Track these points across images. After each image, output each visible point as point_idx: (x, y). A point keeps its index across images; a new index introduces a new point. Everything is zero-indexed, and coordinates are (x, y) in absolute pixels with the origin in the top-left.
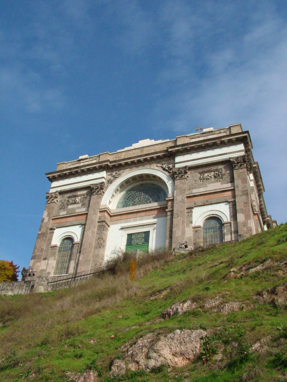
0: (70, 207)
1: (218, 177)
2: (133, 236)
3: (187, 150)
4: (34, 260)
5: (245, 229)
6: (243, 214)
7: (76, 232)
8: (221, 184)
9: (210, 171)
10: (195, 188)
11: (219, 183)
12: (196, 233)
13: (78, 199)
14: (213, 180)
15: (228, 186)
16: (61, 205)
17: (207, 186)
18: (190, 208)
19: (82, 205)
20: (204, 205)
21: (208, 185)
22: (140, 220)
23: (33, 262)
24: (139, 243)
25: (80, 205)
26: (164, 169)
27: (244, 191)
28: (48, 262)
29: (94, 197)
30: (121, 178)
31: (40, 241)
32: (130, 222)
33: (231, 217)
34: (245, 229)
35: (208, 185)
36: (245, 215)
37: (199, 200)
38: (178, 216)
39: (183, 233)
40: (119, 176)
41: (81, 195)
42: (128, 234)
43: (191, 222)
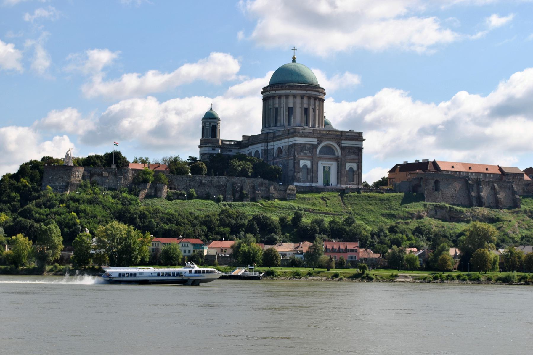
0: (304, 152)
1: (354, 153)
7: (308, 163)
9: (351, 149)
11: (354, 156)
22: (328, 161)
25: (308, 152)
26: (337, 144)
33: (357, 169)
37: (348, 161)
39: (344, 172)
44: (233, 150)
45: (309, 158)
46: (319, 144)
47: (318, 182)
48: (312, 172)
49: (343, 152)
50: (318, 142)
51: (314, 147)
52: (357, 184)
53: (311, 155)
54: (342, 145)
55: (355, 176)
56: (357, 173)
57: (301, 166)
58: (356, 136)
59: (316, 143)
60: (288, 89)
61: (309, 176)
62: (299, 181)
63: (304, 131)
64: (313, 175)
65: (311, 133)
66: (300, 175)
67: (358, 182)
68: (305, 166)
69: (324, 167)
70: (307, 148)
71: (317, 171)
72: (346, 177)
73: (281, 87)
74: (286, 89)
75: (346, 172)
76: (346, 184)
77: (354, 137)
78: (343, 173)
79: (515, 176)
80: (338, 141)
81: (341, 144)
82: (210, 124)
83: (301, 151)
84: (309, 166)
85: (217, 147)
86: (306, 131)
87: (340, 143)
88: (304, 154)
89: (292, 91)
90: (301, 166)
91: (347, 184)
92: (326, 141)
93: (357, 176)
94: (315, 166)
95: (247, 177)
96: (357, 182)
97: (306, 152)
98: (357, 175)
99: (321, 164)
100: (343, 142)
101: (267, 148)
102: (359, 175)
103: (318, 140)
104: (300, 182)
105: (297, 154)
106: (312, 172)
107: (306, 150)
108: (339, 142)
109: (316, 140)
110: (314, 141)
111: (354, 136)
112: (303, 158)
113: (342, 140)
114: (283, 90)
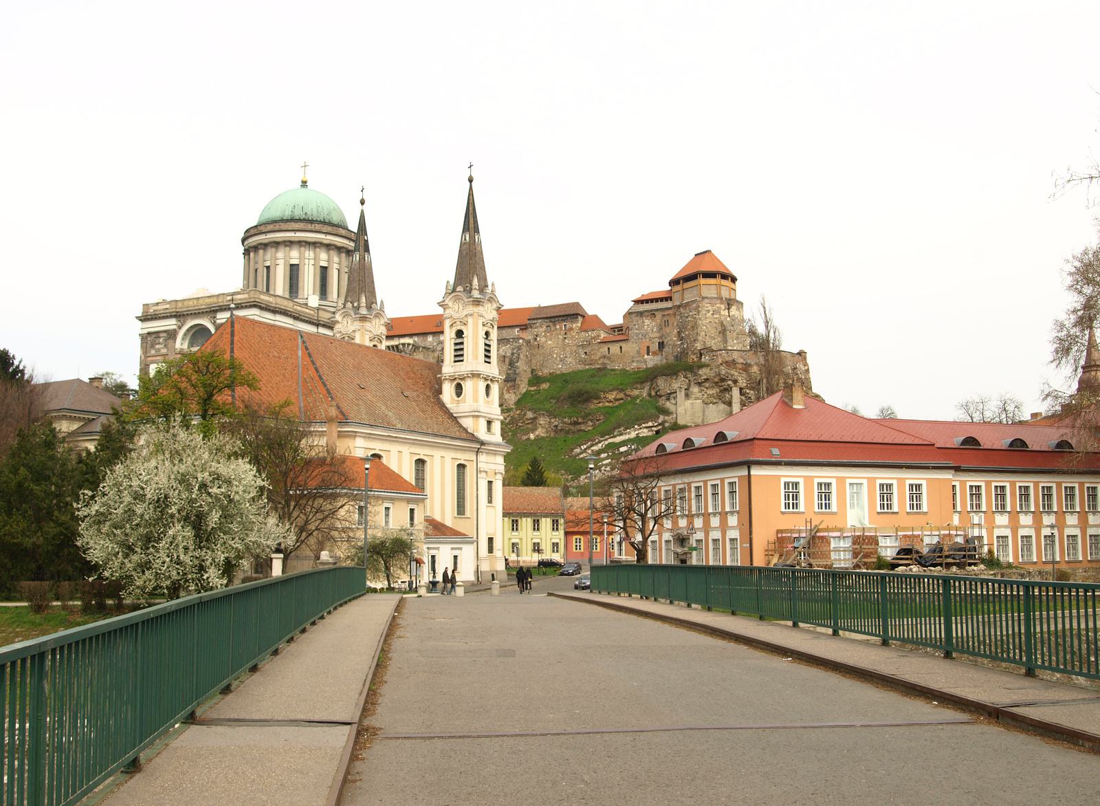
0: (157, 346)
46: (180, 328)
50: (179, 323)
51: (172, 335)
54: (218, 322)
58: (245, 299)
59: (175, 327)
63: (155, 308)
65: (167, 309)
79: (555, 325)
83: (151, 347)
88: (156, 352)
110: (171, 324)
111: (240, 299)
112: (154, 358)
113: (216, 311)
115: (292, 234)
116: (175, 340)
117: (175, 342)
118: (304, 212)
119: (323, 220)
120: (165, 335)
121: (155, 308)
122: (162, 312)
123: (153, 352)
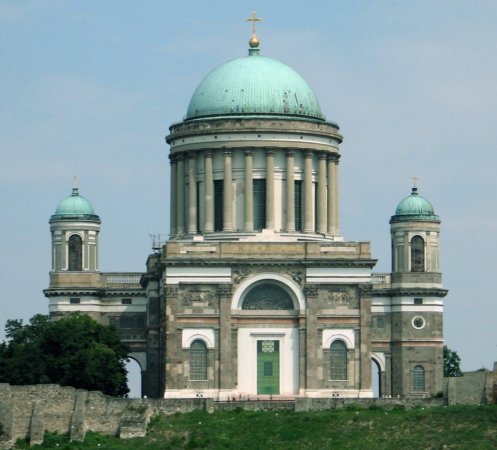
0: (195, 304)
2: (263, 343)
3: (319, 264)
4: (169, 364)
5: (366, 360)
6: (366, 345)
8: (349, 308)
9: (338, 291)
10: (325, 307)
11: (346, 307)
12: (325, 355)
13: (202, 296)
14: (341, 302)
15: (355, 312)
16: (183, 300)
17: (335, 308)
18: (321, 330)
19: (209, 305)
20: (332, 328)
21: (337, 307)
23: (169, 365)
24: (270, 352)
26: (294, 279)
27: (368, 322)
28: (183, 366)
29: (224, 300)
30: (248, 280)
31: (171, 342)
32: (258, 327)
33: (356, 344)
34: (366, 360)
35: (337, 307)
36: (367, 346)
37: (329, 322)
38: (311, 338)
39: (316, 355)
40: (247, 276)
41: (205, 292)
42: (258, 341)
43: (321, 344)
44: (135, 301)
45: (210, 321)
46: (237, 282)
47: (236, 384)
48: (219, 359)
49: (309, 300)
50: (236, 275)
52: (357, 386)
53: (215, 312)
55: (351, 363)
56: (357, 356)
57: (186, 343)
58: (351, 253)
59: (229, 280)
60: (208, 133)
61: (211, 371)
62: (180, 384)
63: (191, 249)
64: (222, 368)
65: (212, 252)
66: (183, 368)
67: (360, 379)
68: (199, 342)
69: (259, 343)
70: (202, 296)
71: (234, 354)
72: (320, 369)
73: (195, 127)
74: (202, 134)
75: (320, 355)
76: (323, 385)
77: (343, 257)
78: (311, 355)
80: (296, 271)
81: (306, 277)
82: (64, 232)
83: (184, 305)
84: (211, 343)
85: (81, 294)
86: (198, 249)
87: (300, 276)
88: (194, 311)
89: (218, 136)
90: (186, 343)
91: (327, 387)
92: (260, 272)
93: (357, 362)
94: (226, 342)
95: (11, 384)
96: (357, 381)
97: (200, 304)
98: (355, 360)
99: (252, 335)
100: (310, 272)
101: (157, 296)
102: (360, 360)
103: (233, 272)
104: (185, 387)
105: (173, 312)
106: (219, 359)
107: (200, 300)
108: (299, 273)
109: (227, 272)
111: (344, 253)
113: (305, 266)
114: (196, 135)
115: (296, 139)
116: (230, 296)
117: (230, 302)
118: (299, 104)
119: (316, 116)
120: (209, 289)
121: (191, 249)
122: (203, 256)
123: (188, 312)
